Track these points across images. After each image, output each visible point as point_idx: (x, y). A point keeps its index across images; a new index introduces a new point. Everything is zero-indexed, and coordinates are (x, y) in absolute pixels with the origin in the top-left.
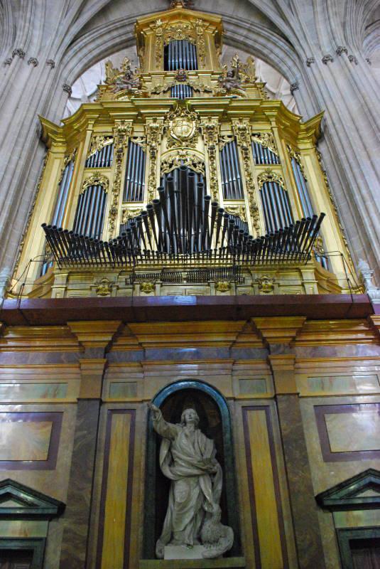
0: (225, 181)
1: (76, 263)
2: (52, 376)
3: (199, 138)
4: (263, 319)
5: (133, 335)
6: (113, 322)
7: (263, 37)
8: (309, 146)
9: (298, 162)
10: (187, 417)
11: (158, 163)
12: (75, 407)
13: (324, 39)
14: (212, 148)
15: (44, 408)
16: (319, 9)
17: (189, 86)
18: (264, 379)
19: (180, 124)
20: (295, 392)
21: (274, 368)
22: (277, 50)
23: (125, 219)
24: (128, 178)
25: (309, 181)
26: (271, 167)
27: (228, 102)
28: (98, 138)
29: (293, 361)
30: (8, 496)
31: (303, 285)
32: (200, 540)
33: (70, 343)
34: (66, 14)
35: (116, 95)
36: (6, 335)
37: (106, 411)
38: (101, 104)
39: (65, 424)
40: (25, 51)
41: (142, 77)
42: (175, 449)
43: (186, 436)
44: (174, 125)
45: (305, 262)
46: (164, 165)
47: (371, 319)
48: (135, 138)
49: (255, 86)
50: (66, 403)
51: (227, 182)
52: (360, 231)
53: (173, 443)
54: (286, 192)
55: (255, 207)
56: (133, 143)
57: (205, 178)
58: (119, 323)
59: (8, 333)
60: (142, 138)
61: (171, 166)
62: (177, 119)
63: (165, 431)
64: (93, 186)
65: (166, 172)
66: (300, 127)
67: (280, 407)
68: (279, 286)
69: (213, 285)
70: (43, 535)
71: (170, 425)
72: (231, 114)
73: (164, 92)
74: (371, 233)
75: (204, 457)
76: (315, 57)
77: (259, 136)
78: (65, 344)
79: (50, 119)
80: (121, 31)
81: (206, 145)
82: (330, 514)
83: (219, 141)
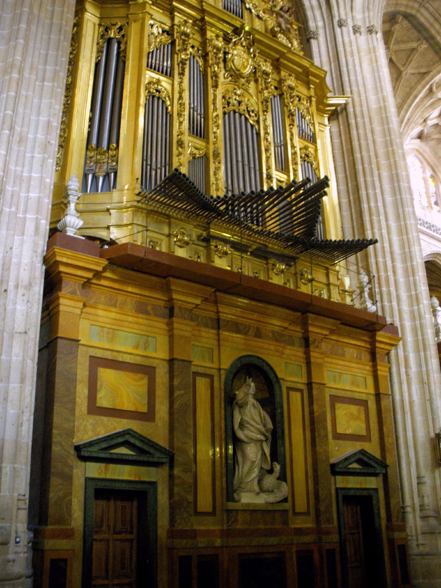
2: (144, 328)
15: (138, 360)
18: (301, 366)
32: (262, 490)
39: (158, 380)
50: (158, 359)
72: (312, 80)
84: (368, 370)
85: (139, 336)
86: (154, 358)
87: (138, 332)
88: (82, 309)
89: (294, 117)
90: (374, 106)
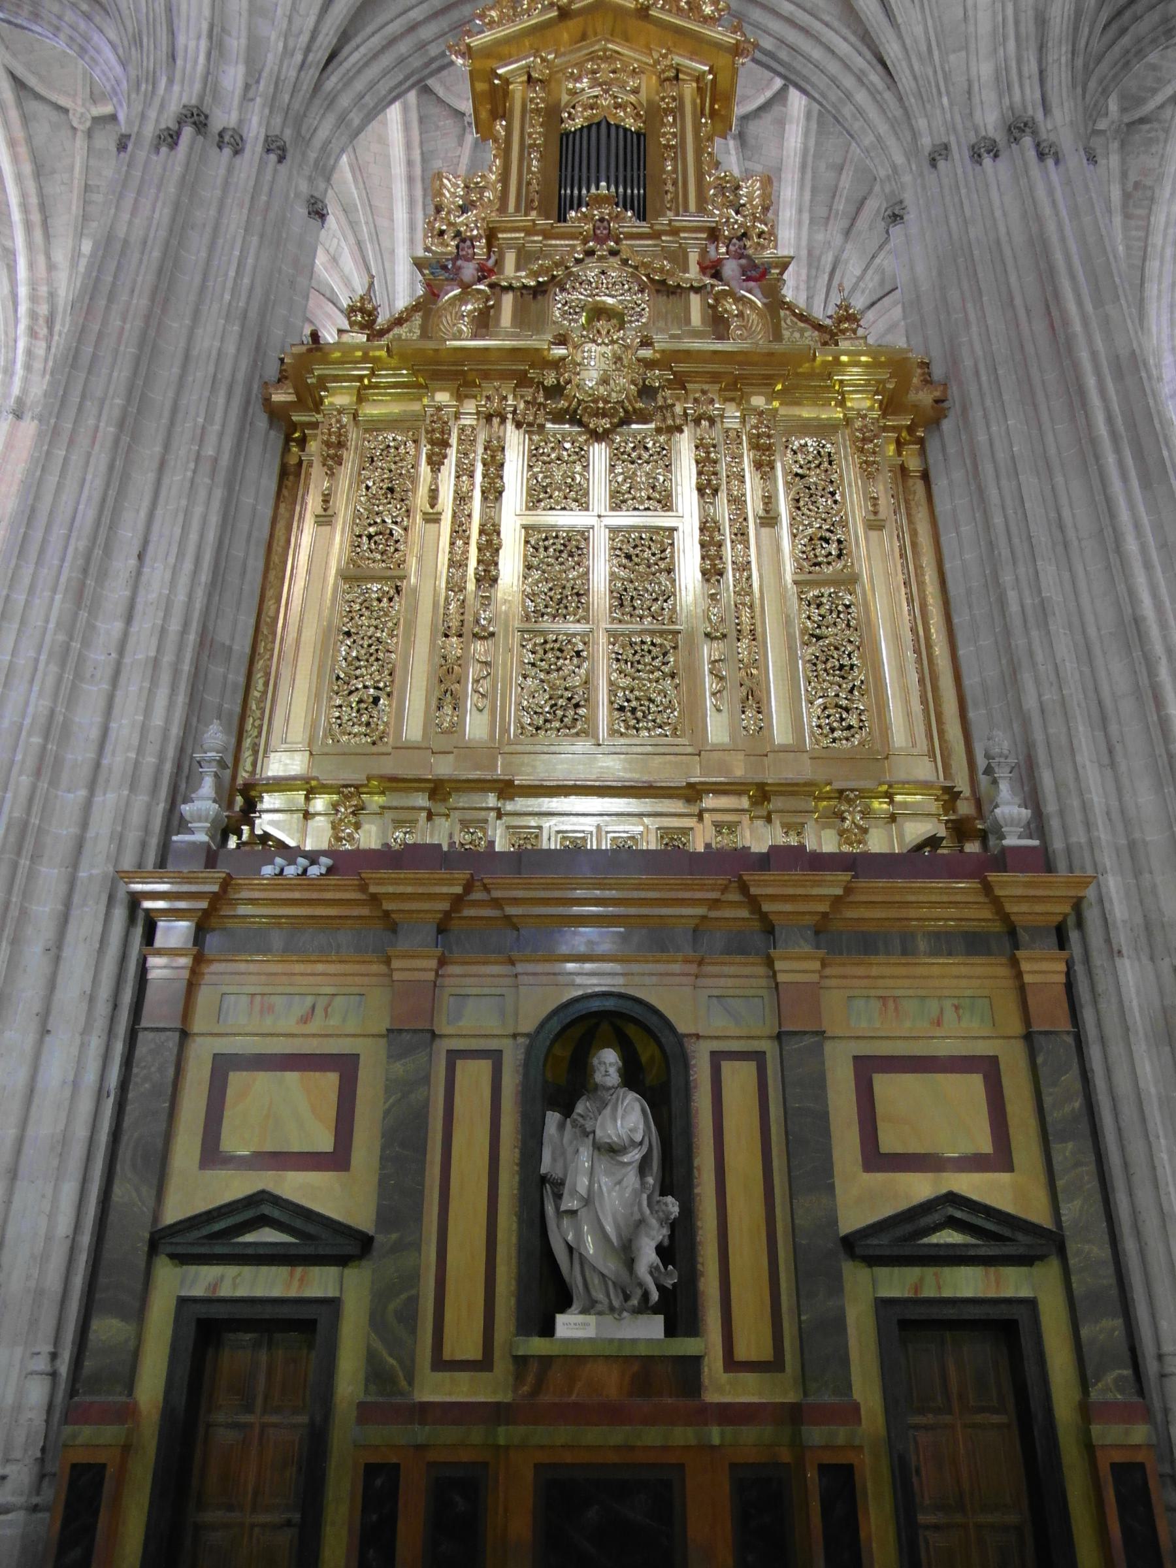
21: (781, 978)
30: (263, 1221)
37: (443, 1055)
70: (331, 1293)
82: (867, 1271)
84: (1004, 977)
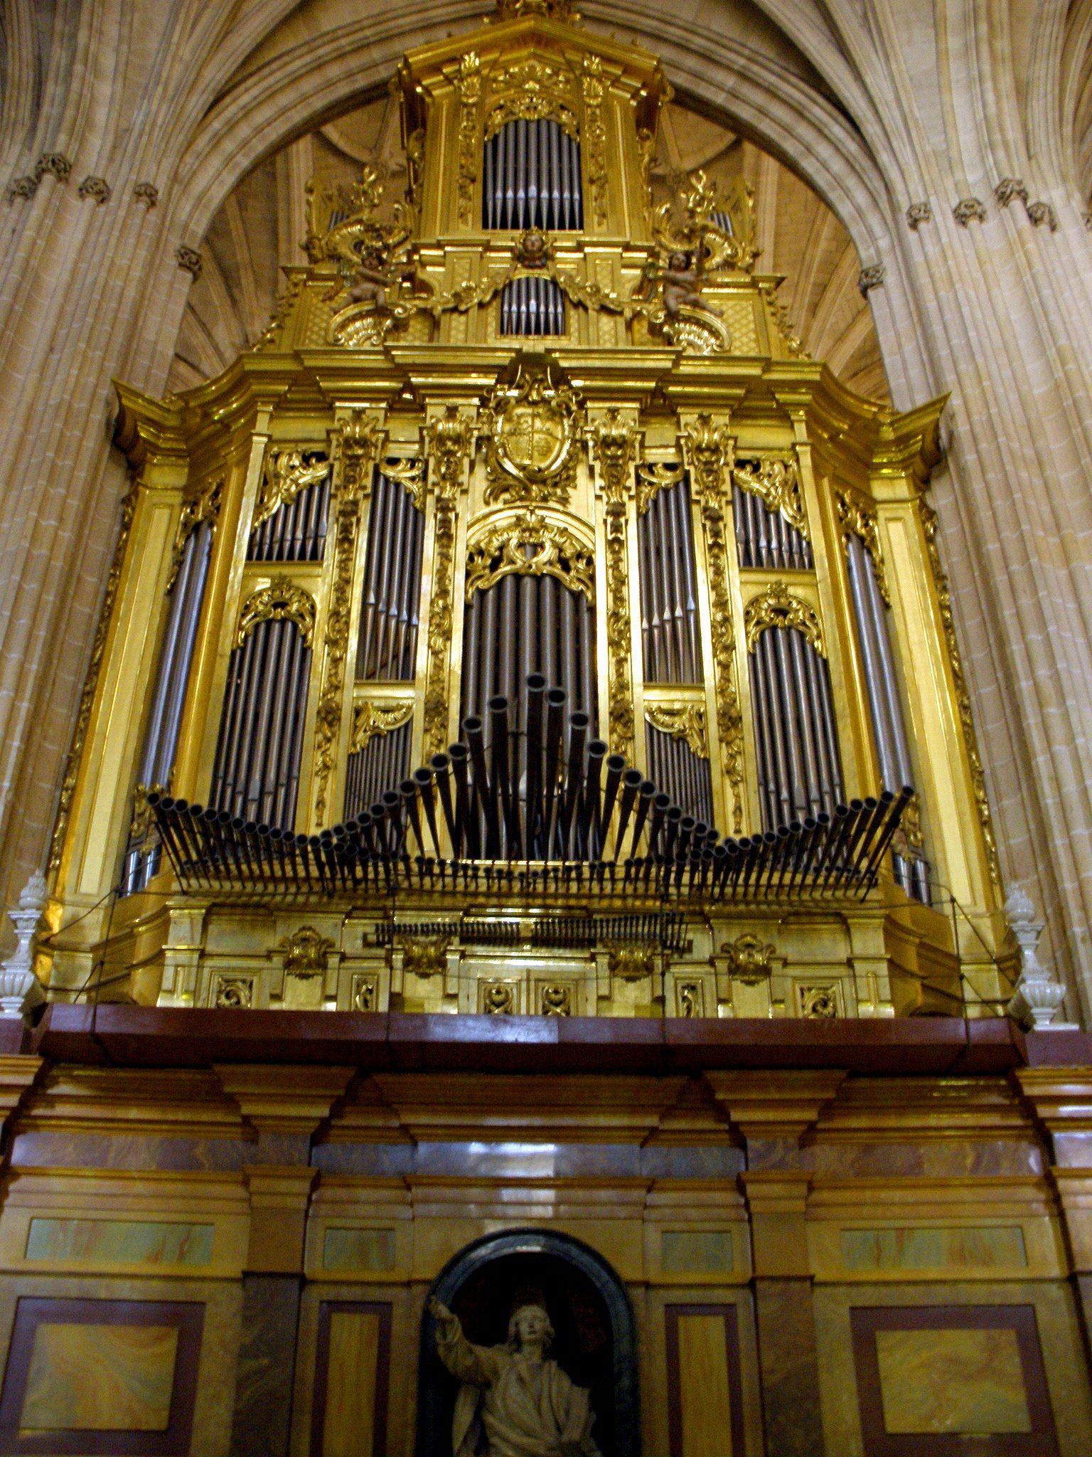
0: (650, 621)
1: (229, 876)
2: (177, 1204)
3: (581, 471)
4: (733, 1075)
5: (386, 1105)
6: (335, 1070)
7: (784, 102)
8: (902, 489)
9: (866, 545)
10: (524, 1328)
11: (460, 554)
12: (236, 1290)
13: (966, 140)
14: (617, 511)
15: (156, 1290)
16: (954, 43)
17: (555, 283)
19: (526, 424)
20: (803, 1273)
21: (755, 1207)
22: (824, 150)
23: (361, 736)
24: (372, 599)
25: (896, 609)
26: (785, 579)
27: (669, 364)
28: (283, 460)
29: (803, 1189)
31: (849, 963)
33: (219, 1117)
34: (193, 28)
35: (338, 319)
36: (52, 1086)
38: (297, 356)
39: (210, 1336)
40: (71, 157)
41: (416, 249)
42: (491, 1412)
43: (521, 1380)
44: (507, 427)
45: (862, 892)
46: (478, 560)
47: (1014, 1076)
48: (393, 462)
49: (754, 284)
51: (656, 621)
52: (1024, 786)
53: (488, 1394)
54: (825, 662)
55: (733, 713)
56: (387, 480)
57: (592, 610)
58: (351, 1072)
59: (55, 1082)
60: (413, 462)
61: (494, 566)
62: (519, 411)
63: (468, 1369)
64: (269, 623)
65: (480, 584)
66: (877, 432)
67: (763, 1311)
68: (786, 963)
69: (603, 961)
71: (483, 1352)
73: (481, 305)
74: (1050, 801)
75: (565, 1438)
76: (933, 199)
77: (756, 468)
78: (205, 1117)
79: (138, 385)
80: (354, 62)
81: (598, 497)
83: (639, 481)
85: (165, 1226)
86: (202, 1279)
87: (162, 1217)
88: (806, 1199)
89: (721, 524)
90: (1039, 388)
